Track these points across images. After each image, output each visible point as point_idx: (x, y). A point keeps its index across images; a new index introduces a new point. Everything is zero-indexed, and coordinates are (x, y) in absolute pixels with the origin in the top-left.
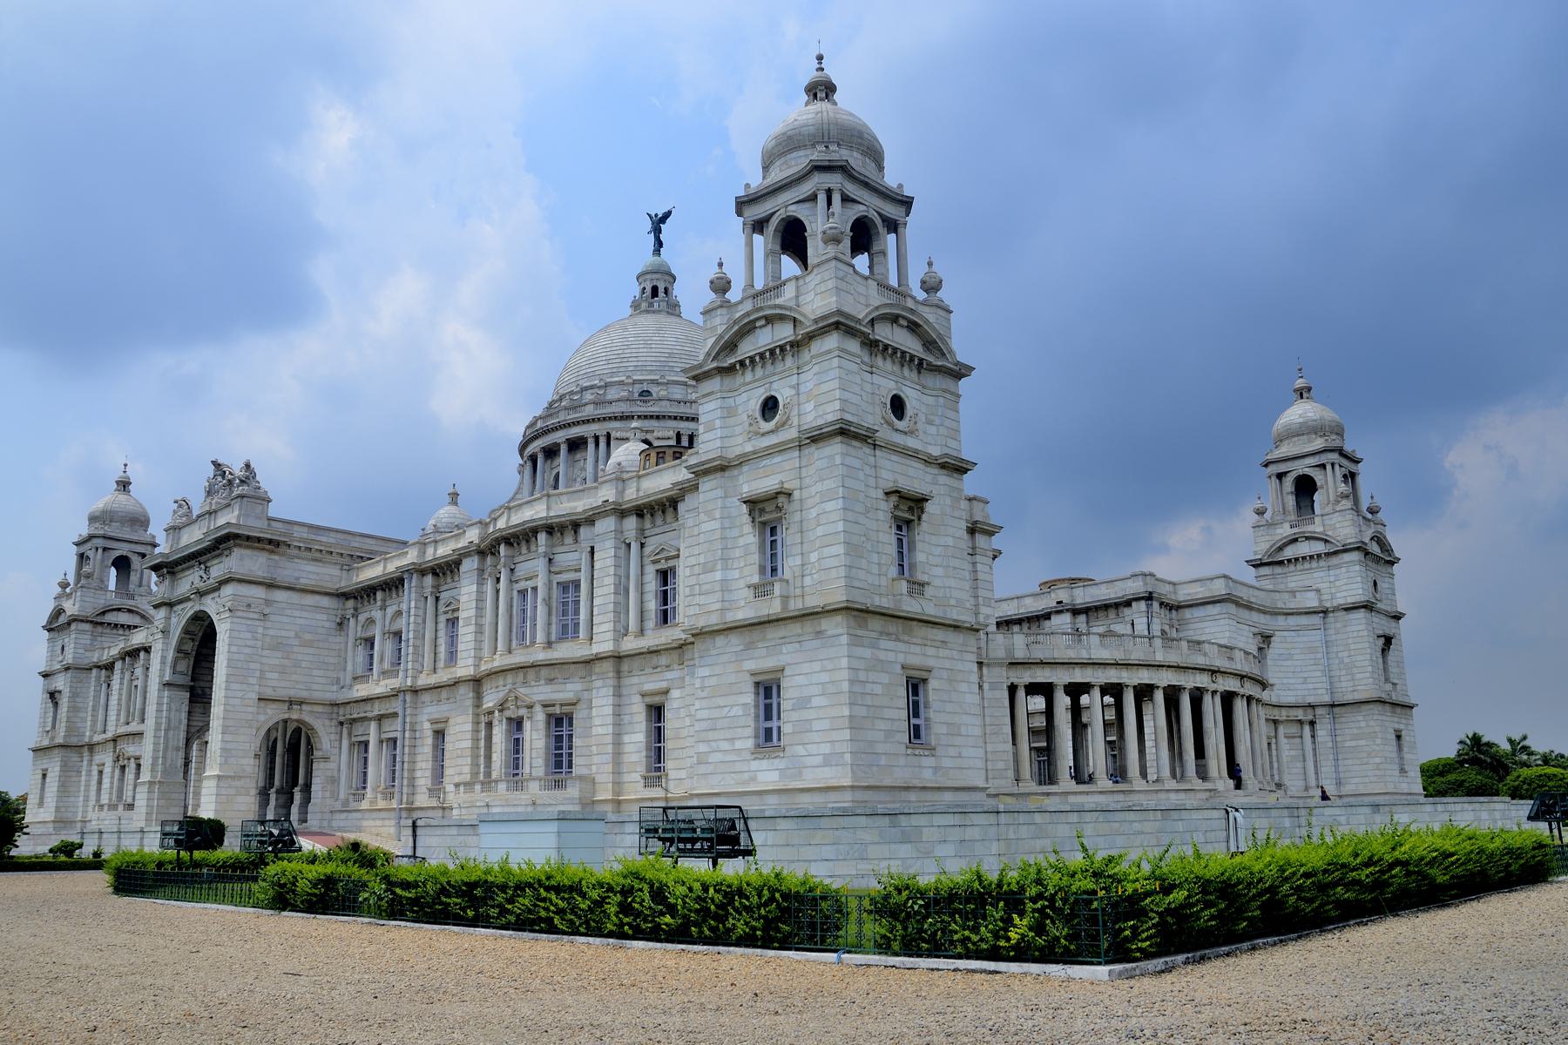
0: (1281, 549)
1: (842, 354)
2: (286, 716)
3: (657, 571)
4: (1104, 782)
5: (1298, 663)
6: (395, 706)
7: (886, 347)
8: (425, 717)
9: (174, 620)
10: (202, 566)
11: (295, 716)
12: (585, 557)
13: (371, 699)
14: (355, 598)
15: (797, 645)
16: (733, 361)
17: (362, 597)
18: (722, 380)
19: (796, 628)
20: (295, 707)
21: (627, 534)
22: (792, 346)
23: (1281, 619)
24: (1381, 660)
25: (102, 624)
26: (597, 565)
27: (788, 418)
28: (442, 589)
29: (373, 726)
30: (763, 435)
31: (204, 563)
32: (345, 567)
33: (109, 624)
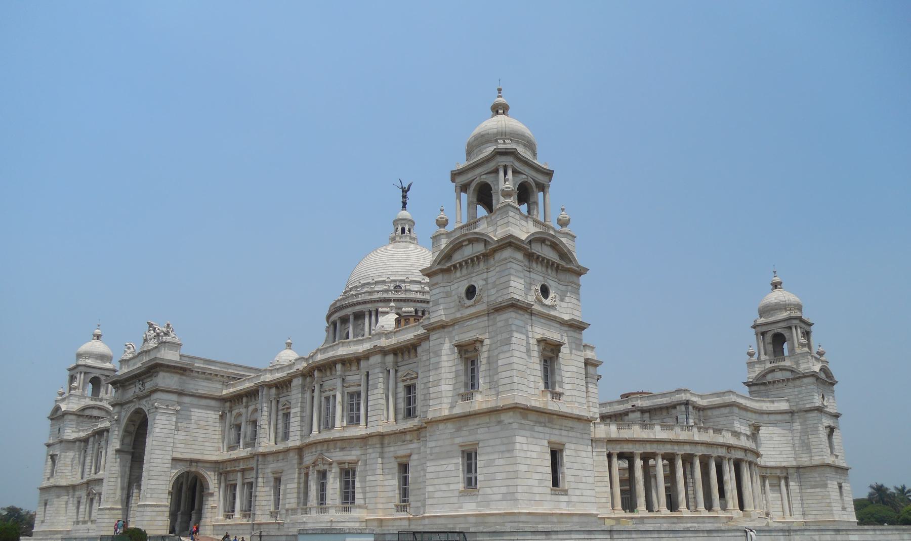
0: (764, 376)
1: (512, 260)
2: (188, 469)
3: (405, 386)
4: (666, 512)
5: (776, 442)
6: (253, 464)
7: (538, 257)
8: (269, 470)
9: (123, 414)
10: (141, 382)
11: (193, 469)
12: (364, 378)
13: (238, 459)
14: (231, 401)
15: (486, 429)
16: (449, 265)
17: (234, 401)
18: (443, 276)
19: (486, 419)
20: (193, 464)
22: (484, 256)
23: (765, 417)
24: (827, 441)
25: (82, 416)
26: (370, 383)
27: (482, 298)
29: (239, 474)
30: (467, 307)
31: (142, 380)
32: (225, 383)
33: (87, 416)
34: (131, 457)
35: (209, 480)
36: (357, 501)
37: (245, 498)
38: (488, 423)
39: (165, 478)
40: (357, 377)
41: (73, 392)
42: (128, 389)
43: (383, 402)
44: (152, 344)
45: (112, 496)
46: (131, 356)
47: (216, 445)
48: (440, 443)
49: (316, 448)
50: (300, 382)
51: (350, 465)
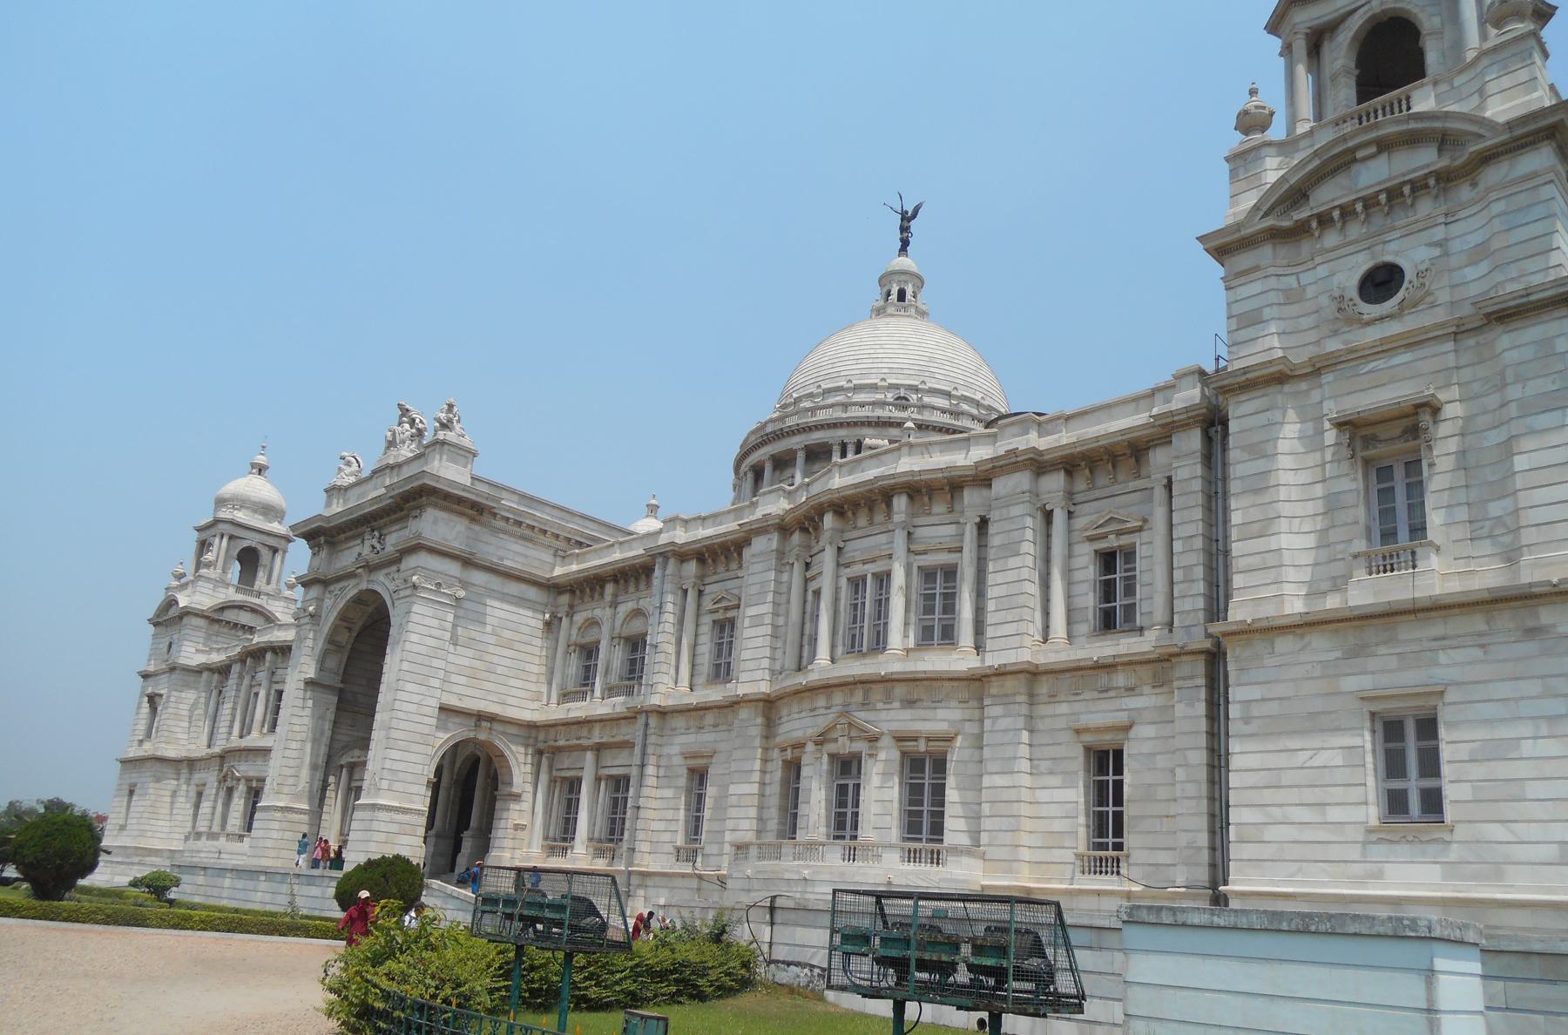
2: (472, 735)
3: (1096, 551)
6: (625, 733)
8: (675, 750)
9: (328, 602)
10: (376, 533)
11: (482, 736)
12: (970, 533)
13: (590, 722)
14: (572, 592)
15: (1478, 653)
20: (484, 724)
21: (1045, 498)
22: (1438, 181)
25: (219, 621)
28: (707, 580)
29: (589, 756)
31: (379, 529)
33: (228, 623)
34: (335, 699)
35: (512, 762)
36: (949, 838)
37: (599, 811)
38: (1480, 635)
39: (421, 748)
40: (951, 530)
41: (203, 571)
42: (342, 551)
43: (1034, 589)
44: (406, 451)
45: (291, 781)
46: (352, 479)
47: (534, 687)
48: (1279, 690)
49: (829, 698)
50: (774, 545)
51: (931, 743)
